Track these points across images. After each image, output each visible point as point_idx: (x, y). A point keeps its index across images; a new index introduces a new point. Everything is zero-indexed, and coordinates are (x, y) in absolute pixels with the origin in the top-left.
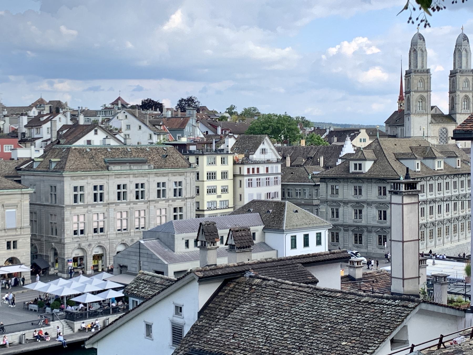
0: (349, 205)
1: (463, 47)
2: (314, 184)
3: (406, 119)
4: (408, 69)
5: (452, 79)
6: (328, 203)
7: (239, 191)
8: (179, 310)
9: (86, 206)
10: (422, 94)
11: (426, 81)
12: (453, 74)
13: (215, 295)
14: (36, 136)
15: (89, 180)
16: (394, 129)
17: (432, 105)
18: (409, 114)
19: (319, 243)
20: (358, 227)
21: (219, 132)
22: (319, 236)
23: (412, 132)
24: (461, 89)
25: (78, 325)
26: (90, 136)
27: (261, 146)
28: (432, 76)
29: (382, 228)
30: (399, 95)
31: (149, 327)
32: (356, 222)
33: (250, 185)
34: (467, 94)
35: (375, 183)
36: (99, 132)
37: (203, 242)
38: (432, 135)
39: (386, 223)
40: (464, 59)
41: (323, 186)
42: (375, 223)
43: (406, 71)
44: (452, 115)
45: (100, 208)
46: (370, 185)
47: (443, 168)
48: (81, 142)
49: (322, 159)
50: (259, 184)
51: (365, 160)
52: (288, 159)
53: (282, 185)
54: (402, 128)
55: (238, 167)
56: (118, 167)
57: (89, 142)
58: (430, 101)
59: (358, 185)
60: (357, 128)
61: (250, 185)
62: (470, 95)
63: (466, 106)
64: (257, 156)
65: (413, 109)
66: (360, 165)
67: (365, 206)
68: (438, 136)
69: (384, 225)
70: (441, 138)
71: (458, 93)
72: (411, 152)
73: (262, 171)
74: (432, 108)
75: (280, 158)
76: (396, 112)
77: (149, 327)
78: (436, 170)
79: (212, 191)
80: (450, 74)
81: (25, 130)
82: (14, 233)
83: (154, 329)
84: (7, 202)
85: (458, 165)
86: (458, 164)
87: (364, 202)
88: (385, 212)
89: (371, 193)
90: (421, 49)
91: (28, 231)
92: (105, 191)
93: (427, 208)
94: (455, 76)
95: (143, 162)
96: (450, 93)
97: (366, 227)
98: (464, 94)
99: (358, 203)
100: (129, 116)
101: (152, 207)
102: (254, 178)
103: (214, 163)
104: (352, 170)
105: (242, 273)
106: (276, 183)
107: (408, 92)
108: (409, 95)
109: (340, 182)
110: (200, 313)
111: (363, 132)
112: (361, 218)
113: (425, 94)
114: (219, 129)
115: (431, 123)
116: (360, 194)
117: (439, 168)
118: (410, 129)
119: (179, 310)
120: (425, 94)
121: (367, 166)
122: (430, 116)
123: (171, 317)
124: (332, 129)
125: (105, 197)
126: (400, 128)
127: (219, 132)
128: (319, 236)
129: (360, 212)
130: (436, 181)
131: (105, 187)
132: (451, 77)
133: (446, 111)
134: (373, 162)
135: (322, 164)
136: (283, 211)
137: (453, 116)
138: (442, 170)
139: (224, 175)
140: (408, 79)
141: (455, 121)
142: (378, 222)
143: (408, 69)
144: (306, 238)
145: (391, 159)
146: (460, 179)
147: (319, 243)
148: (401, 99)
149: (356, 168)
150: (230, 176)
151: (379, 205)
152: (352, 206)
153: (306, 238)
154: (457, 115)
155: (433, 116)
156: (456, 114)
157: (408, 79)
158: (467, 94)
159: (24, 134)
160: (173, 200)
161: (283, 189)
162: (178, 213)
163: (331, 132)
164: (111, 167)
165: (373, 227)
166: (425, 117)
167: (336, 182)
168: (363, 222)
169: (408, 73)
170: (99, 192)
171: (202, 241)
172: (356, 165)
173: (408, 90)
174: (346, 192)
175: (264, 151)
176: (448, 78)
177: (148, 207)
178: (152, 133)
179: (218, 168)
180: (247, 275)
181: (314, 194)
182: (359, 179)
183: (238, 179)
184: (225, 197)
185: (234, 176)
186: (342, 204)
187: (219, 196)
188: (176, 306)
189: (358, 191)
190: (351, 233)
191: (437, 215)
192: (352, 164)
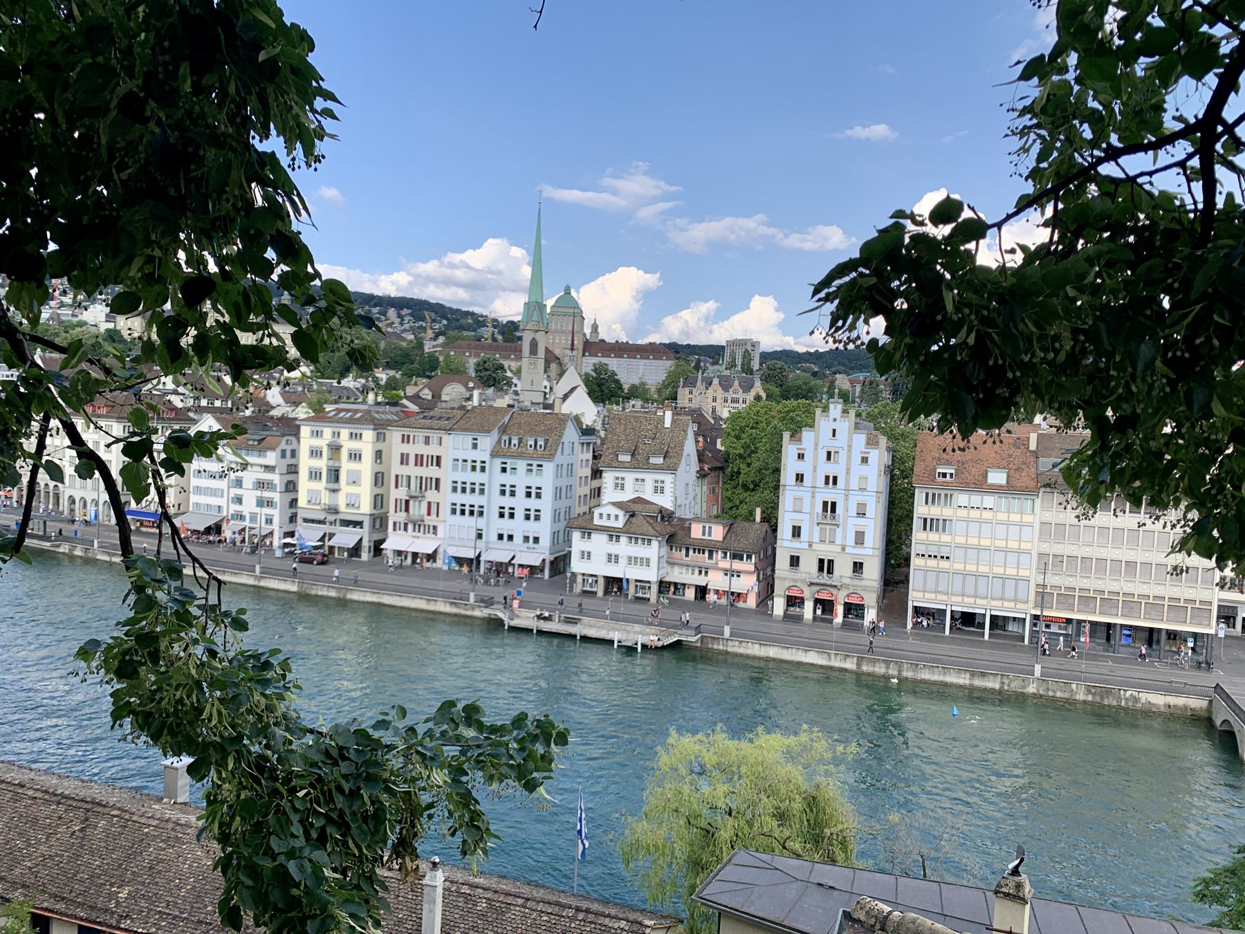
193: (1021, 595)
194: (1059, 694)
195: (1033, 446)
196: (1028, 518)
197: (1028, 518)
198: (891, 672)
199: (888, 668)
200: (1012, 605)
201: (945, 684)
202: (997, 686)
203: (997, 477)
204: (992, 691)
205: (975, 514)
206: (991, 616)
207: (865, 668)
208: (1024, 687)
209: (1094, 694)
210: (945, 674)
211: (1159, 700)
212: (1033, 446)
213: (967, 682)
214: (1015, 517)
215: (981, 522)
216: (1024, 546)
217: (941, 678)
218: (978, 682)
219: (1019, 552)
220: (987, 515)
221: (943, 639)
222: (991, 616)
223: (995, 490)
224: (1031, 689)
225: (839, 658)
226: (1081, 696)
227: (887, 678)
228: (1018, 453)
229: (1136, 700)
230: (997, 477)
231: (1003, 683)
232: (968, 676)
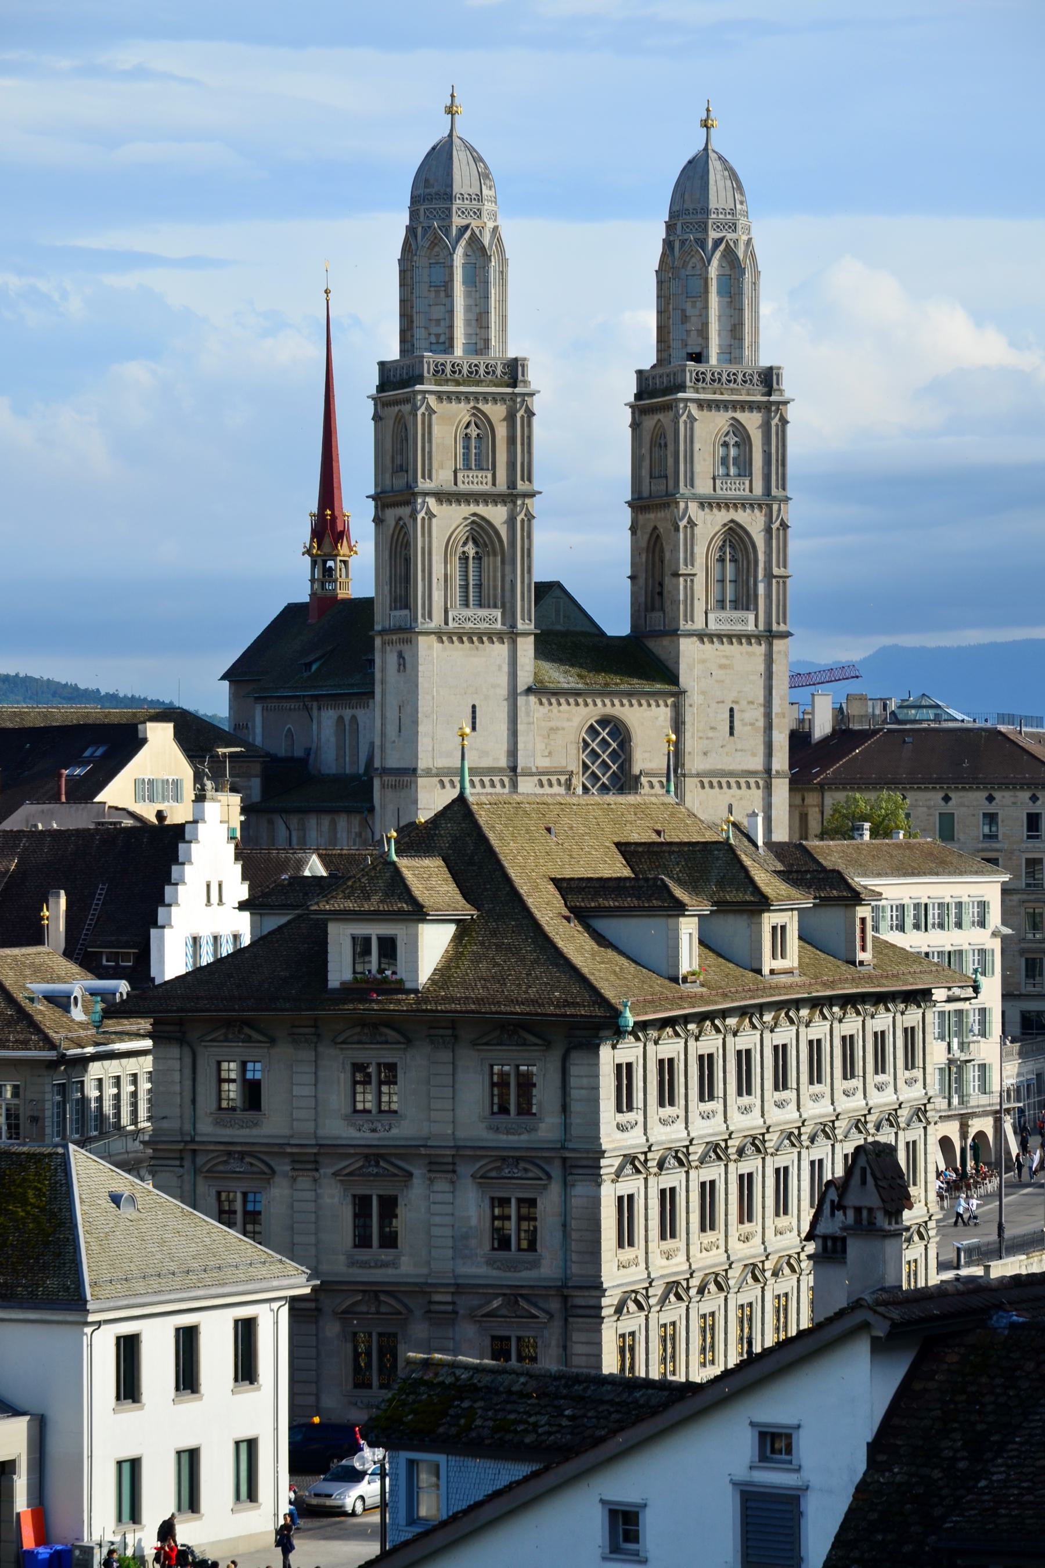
0: (327, 1171)
1: (713, 235)
2: (51, 1055)
3: (385, 660)
4: (392, 352)
5: (649, 422)
6: (200, 1160)
8: (775, 1443)
10: (482, 510)
11: (501, 431)
12: (654, 397)
17: (541, 573)
18: (406, 633)
19: (246, 1370)
20: (374, 1292)
22: (246, 1333)
23: (424, 744)
24: (703, 486)
28: (537, 404)
30: (314, 507)
32: (364, 1265)
34: (742, 517)
35: (474, 1044)
37: (865, 1213)
38: (543, 763)
39: (535, 1264)
42: (477, 1268)
43: (382, 365)
44: (653, 645)
46: (445, 1056)
47: (796, 964)
54: (347, 713)
58: (528, 553)
60: (116, 714)
62: (753, 522)
63: (729, 588)
66: (388, 947)
67: (416, 1172)
68: (575, 766)
69: (525, 1276)
70: (594, 777)
72: (627, 872)
76: (292, 613)
78: (766, 971)
80: (638, 396)
85: (864, 949)
86: (863, 939)
87: (409, 1151)
90: (475, 242)
94: (667, 407)
96: (640, 504)
97: (422, 1290)
98: (722, 517)
99: (375, 1157)
104: (340, 969)
107: (396, 496)
108: (404, 511)
109: (272, 1041)
110: (874, 1448)
111: (160, 736)
112: (390, 1241)
113: (497, 514)
117: (779, 964)
118: (416, 723)
119: (775, 1443)
120: (497, 514)
122: (526, 647)
123: (742, 1473)
126: (327, 719)
128: (246, 1333)
129: (389, 1206)
130: (767, 1035)
133: (615, 619)
134: (452, 928)
137: (657, 646)
138: (789, 972)
140: (400, 419)
141: (673, 678)
142: (490, 1263)
143: (392, 352)
144: (187, 1341)
145: (547, 908)
146: (869, 1022)
147: (246, 1370)
148: (328, 531)
152: (344, 1177)
153: (187, 1341)
154: (688, 647)
156: (674, 633)
157: (400, 419)
158: (742, 517)
165: (459, 1288)
167: (249, 1039)
168: (407, 1266)
171: (858, 1210)
172: (361, 947)
173: (399, 483)
176: (627, 415)
181: (48, 1113)
186: (283, 1167)
188: (762, 1435)
191: (769, 1222)
192: (340, 939)
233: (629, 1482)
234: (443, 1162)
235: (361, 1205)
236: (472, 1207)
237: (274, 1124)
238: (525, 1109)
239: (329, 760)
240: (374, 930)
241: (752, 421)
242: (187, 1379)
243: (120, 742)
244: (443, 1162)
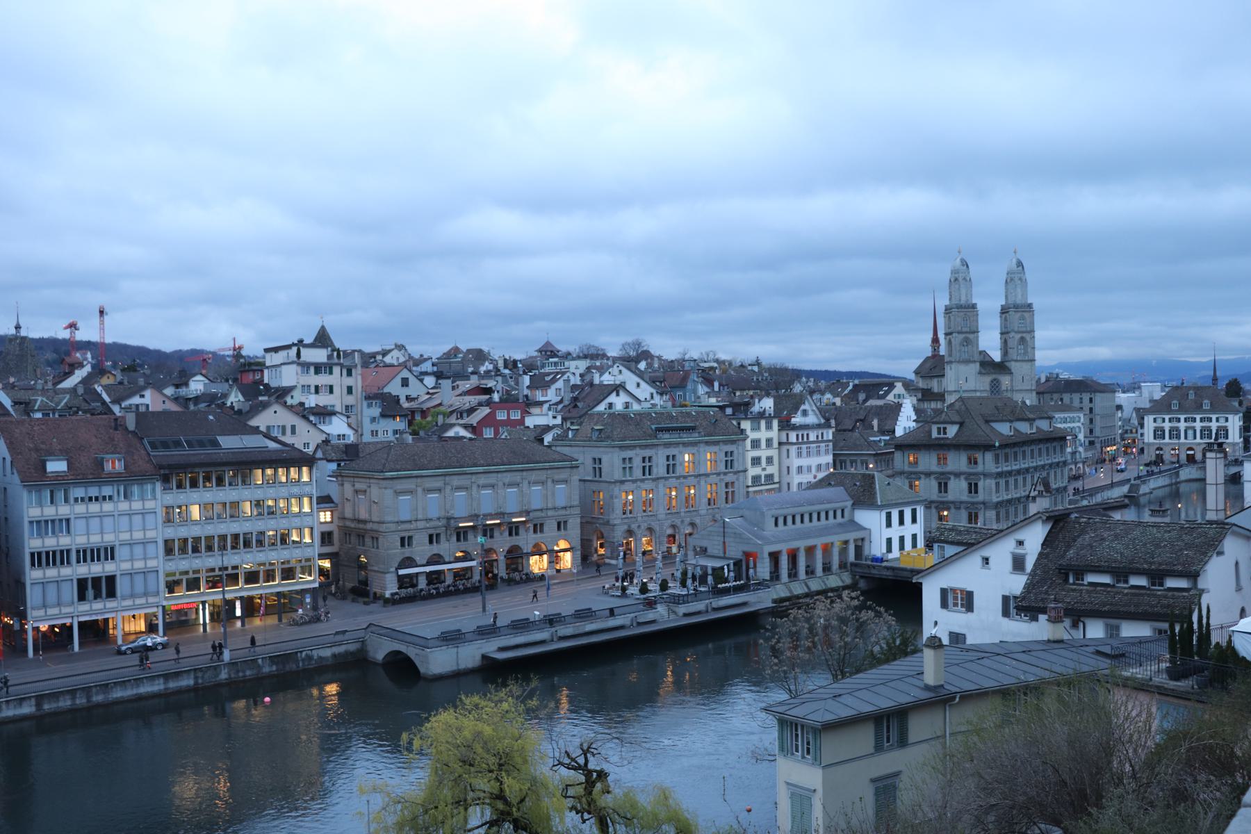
4: (947, 303)
7: (786, 462)
8: (1021, 543)
9: (634, 481)
12: (1004, 311)
13: (1050, 532)
14: (542, 399)
15: (638, 451)
16: (928, 381)
19: (914, 520)
21: (716, 388)
25: (682, 609)
26: (612, 398)
27: (803, 407)
29: (973, 503)
31: (986, 561)
33: (799, 455)
36: (621, 393)
40: (1019, 290)
41: (898, 456)
45: (649, 485)
48: (601, 408)
49: (875, 423)
50: (809, 454)
51: (953, 423)
52: (833, 422)
53: (834, 455)
55: (784, 434)
56: (667, 436)
57: (611, 405)
59: (941, 452)
61: (799, 455)
62: (1027, 337)
64: (797, 420)
65: (956, 355)
71: (1012, 335)
73: (812, 437)
74: (981, 352)
75: (823, 421)
76: (928, 358)
77: (986, 561)
79: (756, 461)
81: (526, 392)
82: (563, 512)
83: (991, 561)
84: (556, 477)
88: (976, 485)
89: (958, 461)
91: (577, 511)
92: (654, 463)
93: (1020, 479)
95: (693, 429)
96: (1002, 334)
99: (942, 474)
100: (624, 370)
101: (703, 483)
102: (804, 446)
103: (759, 428)
104: (935, 435)
105: (1069, 514)
106: (827, 452)
110: (1043, 545)
111: (899, 385)
114: (716, 384)
115: (980, 373)
116: (945, 464)
120: (971, 336)
121: (952, 431)
124: (857, 382)
125: (654, 470)
127: (716, 388)
129: (946, 484)
131: (654, 458)
132: (1002, 313)
133: (997, 356)
135: (876, 428)
136: (873, 483)
139: (769, 442)
144: (901, 514)
147: (914, 520)
148: (935, 340)
149: (939, 433)
150: (775, 444)
151: (968, 476)
152: (936, 478)
155: (983, 364)
159: (527, 396)
160: (725, 474)
161: (834, 461)
162: (730, 490)
163: (855, 386)
164: (660, 435)
165: (961, 502)
166: (972, 365)
169: (948, 310)
170: (647, 464)
174: (928, 461)
175: (805, 413)
177: (699, 483)
178: (654, 391)
179: (763, 434)
180: (1073, 516)
182: (942, 446)
183: (784, 448)
184: (770, 470)
185: (780, 444)
187: (764, 469)
189: (942, 460)
190: (934, 510)
192: (934, 429)
193: (152, 588)
194: (248, 673)
195: (131, 425)
196: (150, 505)
197: (150, 505)
198: (78, 702)
199: (74, 698)
200: (143, 601)
201: (140, 698)
202: (191, 682)
203: (114, 465)
204: (188, 690)
205: (94, 507)
206: (80, 623)
207: (46, 707)
208: (217, 675)
209: (277, 664)
210: (138, 686)
211: (327, 653)
212: (131, 425)
213: (162, 687)
214: (137, 505)
215: (101, 516)
216: (151, 534)
217: (135, 692)
218: (173, 685)
219: (144, 543)
220: (108, 507)
221: (74, 658)
222: (80, 623)
223: (114, 479)
224: (224, 675)
225: (12, 705)
226: (266, 670)
227: (73, 711)
228: (118, 435)
229: (309, 658)
230: (114, 465)
231: (196, 678)
232: (162, 681)
233: (986, 552)
234: (957, 475)
235: (940, 484)
236: (964, 484)
237: (921, 468)
238: (976, 463)
239: (936, 390)
240: (942, 426)
241: (1026, 315)
242: (901, 522)
243: (891, 386)
244: (957, 475)
